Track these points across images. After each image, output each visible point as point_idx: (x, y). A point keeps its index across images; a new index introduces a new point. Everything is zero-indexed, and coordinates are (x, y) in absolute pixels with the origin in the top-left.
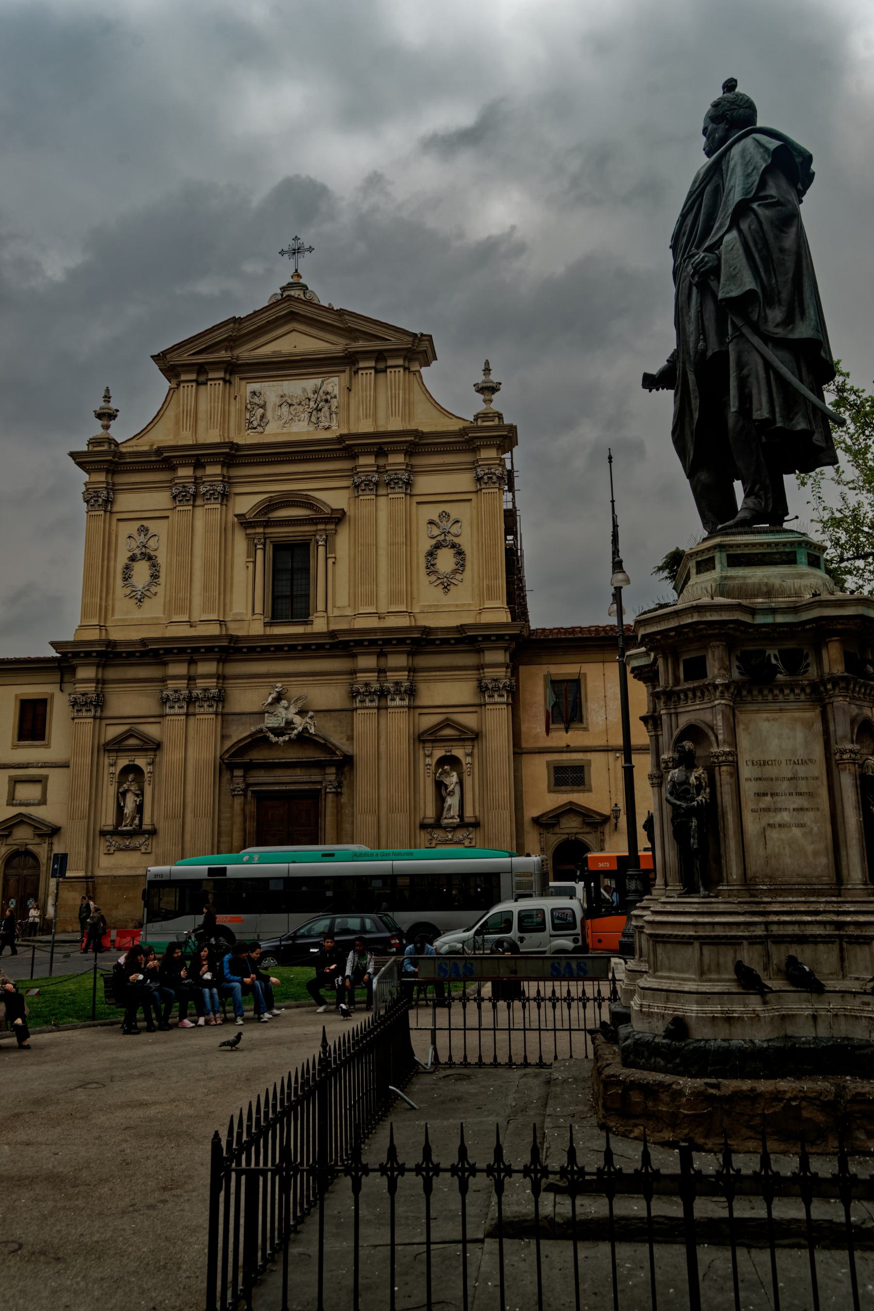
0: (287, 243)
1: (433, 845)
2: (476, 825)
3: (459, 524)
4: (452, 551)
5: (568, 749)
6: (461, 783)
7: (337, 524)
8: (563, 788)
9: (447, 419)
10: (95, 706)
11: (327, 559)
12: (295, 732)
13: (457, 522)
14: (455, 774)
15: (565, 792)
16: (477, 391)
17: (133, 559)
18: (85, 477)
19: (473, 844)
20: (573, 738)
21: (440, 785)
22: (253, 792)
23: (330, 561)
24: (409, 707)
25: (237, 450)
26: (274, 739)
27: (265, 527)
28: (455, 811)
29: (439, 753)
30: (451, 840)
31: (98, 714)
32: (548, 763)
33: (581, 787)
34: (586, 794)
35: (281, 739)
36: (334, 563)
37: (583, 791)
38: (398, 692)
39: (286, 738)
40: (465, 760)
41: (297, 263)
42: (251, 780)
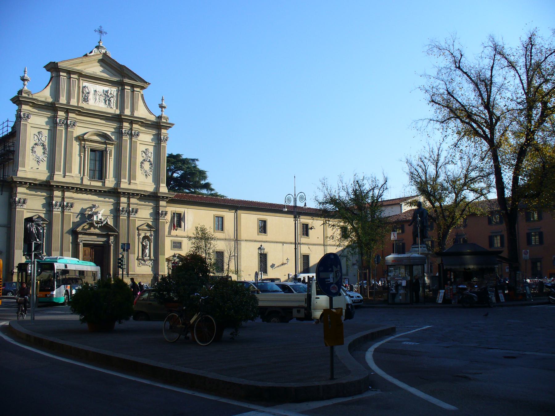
0: (97, 28)
4: (149, 163)
5: (177, 236)
8: (175, 249)
9: (150, 115)
11: (109, 158)
12: (104, 223)
15: (176, 250)
16: (160, 107)
17: (36, 144)
20: (179, 232)
23: (110, 159)
26: (96, 225)
32: (171, 241)
33: (180, 249)
34: (181, 251)
35: (98, 225)
37: (181, 250)
39: (100, 225)
41: (101, 37)
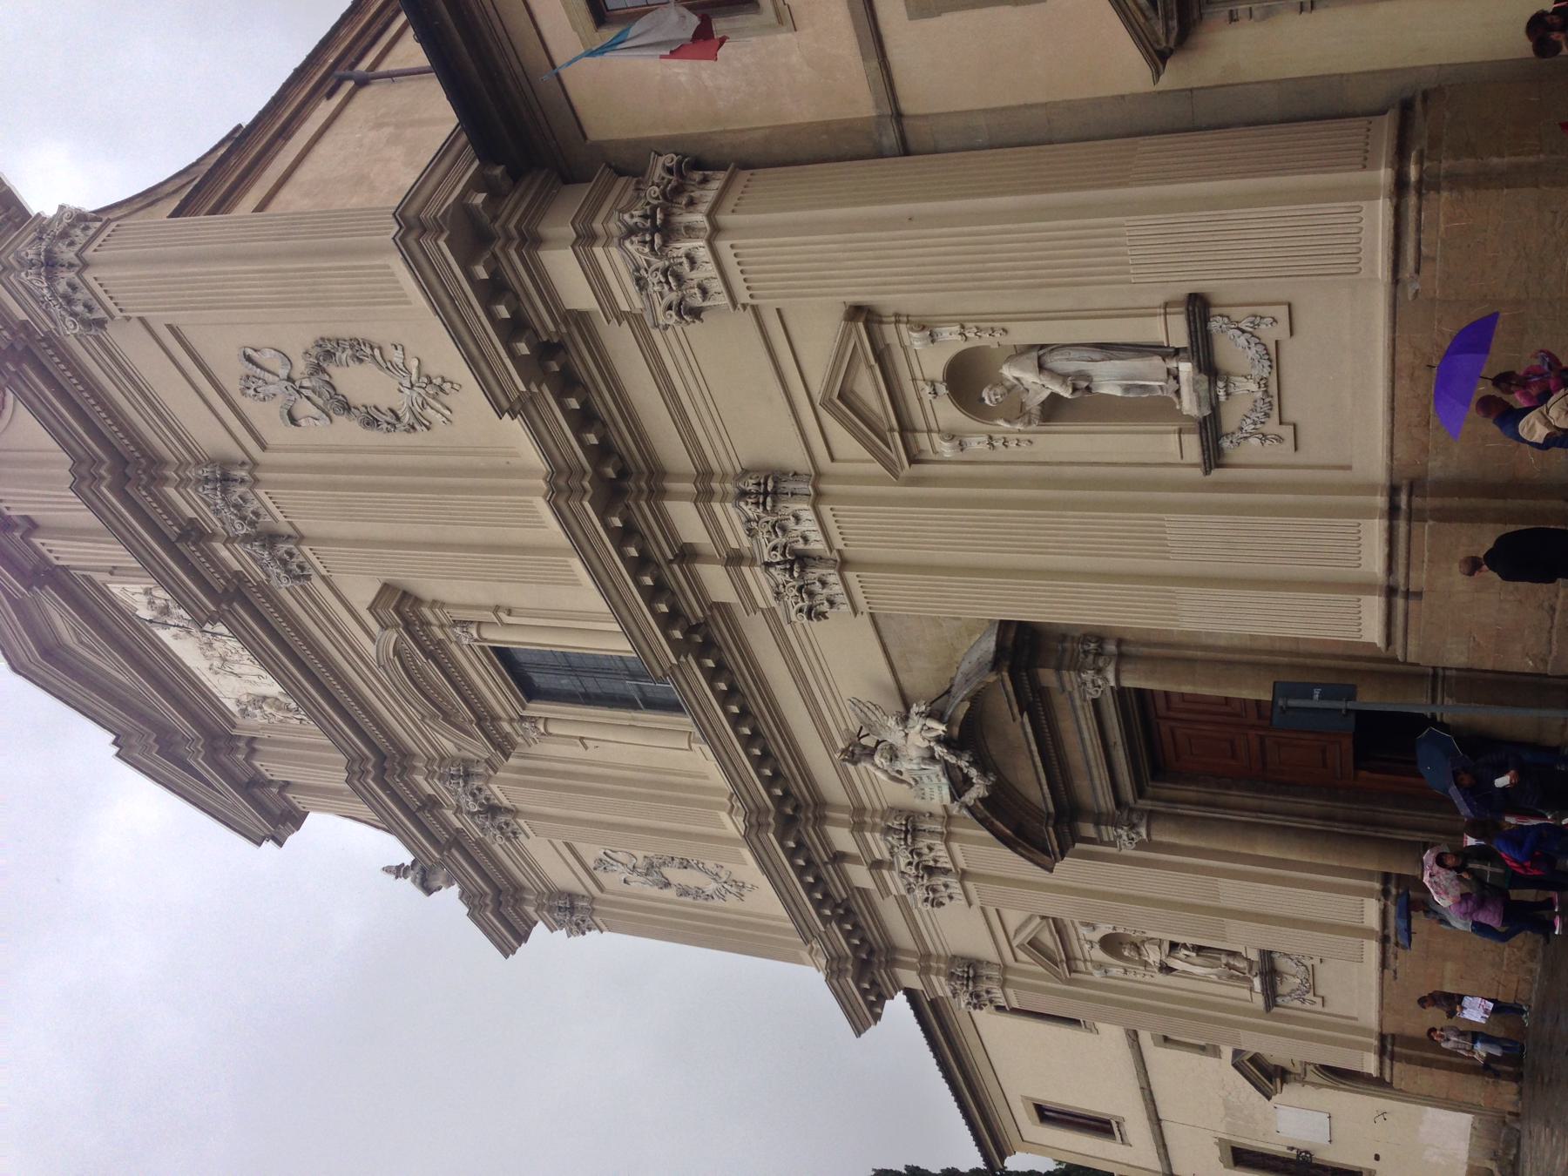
1: (1287, 432)
2: (1198, 308)
3: (249, 352)
4: (331, 368)
6: (1039, 354)
7: (418, 601)
10: (976, 978)
13: (249, 359)
14: (1009, 372)
18: (540, 930)
19: (1282, 313)
21: (1053, 409)
22: (1140, 793)
24: (818, 497)
25: (364, 759)
27: (495, 718)
28: (1150, 370)
29: (947, 412)
30: (1263, 383)
31: (995, 974)
36: (510, 612)
38: (779, 527)
40: (952, 342)
42: (1106, 802)
